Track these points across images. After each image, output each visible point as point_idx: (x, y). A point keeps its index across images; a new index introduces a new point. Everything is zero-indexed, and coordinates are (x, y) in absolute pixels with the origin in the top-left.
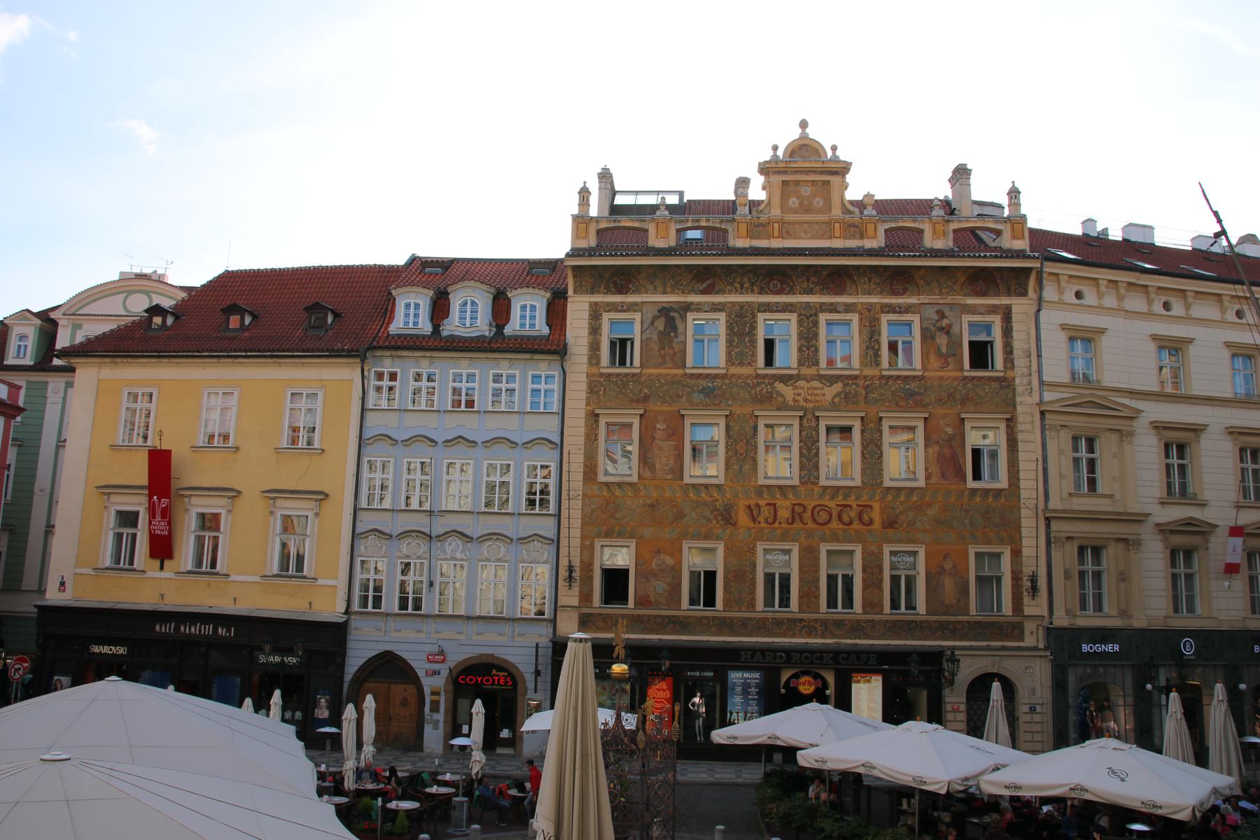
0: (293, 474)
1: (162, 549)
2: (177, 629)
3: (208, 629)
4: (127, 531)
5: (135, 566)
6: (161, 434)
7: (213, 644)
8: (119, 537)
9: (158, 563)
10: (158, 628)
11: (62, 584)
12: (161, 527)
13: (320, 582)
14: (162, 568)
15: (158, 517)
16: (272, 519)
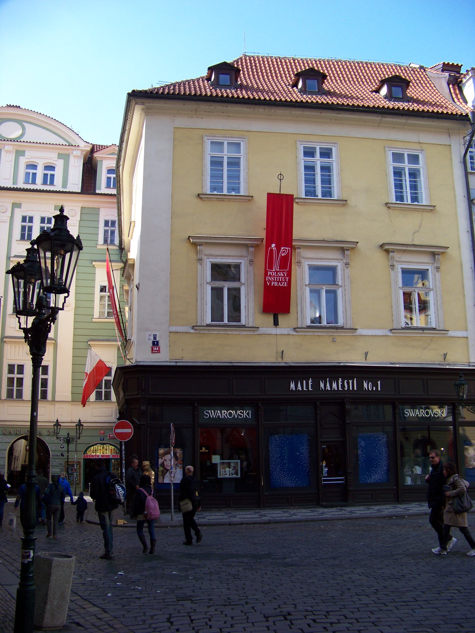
0: (405, 228)
1: (277, 302)
2: (316, 385)
3: (352, 385)
4: (226, 286)
5: (243, 322)
6: (281, 177)
7: (362, 399)
8: (217, 293)
9: (270, 319)
10: (292, 386)
11: (155, 343)
12: (277, 278)
13: (451, 333)
14: (276, 323)
15: (276, 267)
16: (392, 272)
